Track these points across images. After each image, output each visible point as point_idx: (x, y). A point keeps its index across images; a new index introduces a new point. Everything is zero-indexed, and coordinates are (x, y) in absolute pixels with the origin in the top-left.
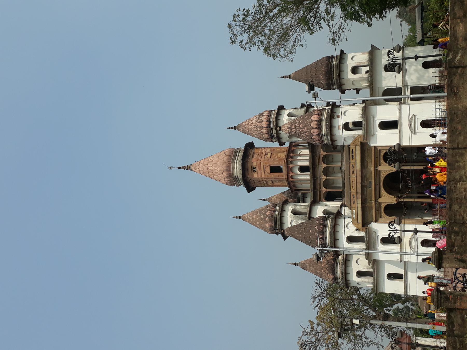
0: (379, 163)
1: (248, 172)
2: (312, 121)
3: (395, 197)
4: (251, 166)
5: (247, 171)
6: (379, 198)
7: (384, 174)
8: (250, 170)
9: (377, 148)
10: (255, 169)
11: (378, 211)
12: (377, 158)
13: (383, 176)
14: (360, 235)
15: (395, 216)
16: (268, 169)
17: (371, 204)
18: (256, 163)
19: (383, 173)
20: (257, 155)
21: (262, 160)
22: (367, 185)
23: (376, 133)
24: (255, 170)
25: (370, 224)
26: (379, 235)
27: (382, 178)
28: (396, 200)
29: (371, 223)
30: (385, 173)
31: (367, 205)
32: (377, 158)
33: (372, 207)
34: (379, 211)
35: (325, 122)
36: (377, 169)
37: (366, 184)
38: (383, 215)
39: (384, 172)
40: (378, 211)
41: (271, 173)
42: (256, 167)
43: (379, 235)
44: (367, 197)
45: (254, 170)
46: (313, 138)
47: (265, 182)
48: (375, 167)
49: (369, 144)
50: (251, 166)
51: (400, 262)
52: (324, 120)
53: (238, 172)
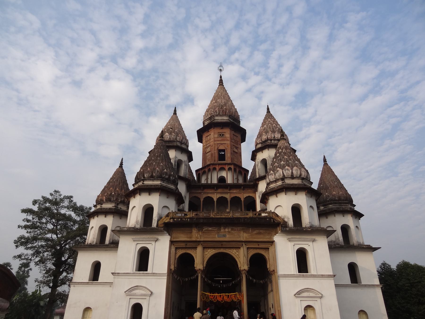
0: (251, 248)
2: (300, 169)
3: (204, 268)
4: (225, 132)
7: (236, 254)
8: (221, 131)
9: (271, 245)
10: (222, 136)
11: (186, 244)
14: (153, 222)
15: (177, 267)
16: (221, 148)
17: (196, 236)
20: (235, 139)
21: (231, 142)
22: (221, 231)
23: (293, 243)
25: (168, 234)
26: (152, 245)
27: (230, 250)
28: (200, 269)
29: (169, 236)
30: (237, 255)
32: (258, 245)
33: (191, 238)
35: (301, 183)
36: (242, 245)
37: (222, 230)
38: (180, 251)
40: (186, 244)
41: (218, 150)
42: (225, 137)
43: (152, 245)
44: (204, 231)
45: (221, 135)
46: (278, 169)
47: (208, 145)
48: (246, 242)
49: (276, 235)
50: (225, 132)
51: (112, 273)
52: (302, 182)
53: (219, 119)
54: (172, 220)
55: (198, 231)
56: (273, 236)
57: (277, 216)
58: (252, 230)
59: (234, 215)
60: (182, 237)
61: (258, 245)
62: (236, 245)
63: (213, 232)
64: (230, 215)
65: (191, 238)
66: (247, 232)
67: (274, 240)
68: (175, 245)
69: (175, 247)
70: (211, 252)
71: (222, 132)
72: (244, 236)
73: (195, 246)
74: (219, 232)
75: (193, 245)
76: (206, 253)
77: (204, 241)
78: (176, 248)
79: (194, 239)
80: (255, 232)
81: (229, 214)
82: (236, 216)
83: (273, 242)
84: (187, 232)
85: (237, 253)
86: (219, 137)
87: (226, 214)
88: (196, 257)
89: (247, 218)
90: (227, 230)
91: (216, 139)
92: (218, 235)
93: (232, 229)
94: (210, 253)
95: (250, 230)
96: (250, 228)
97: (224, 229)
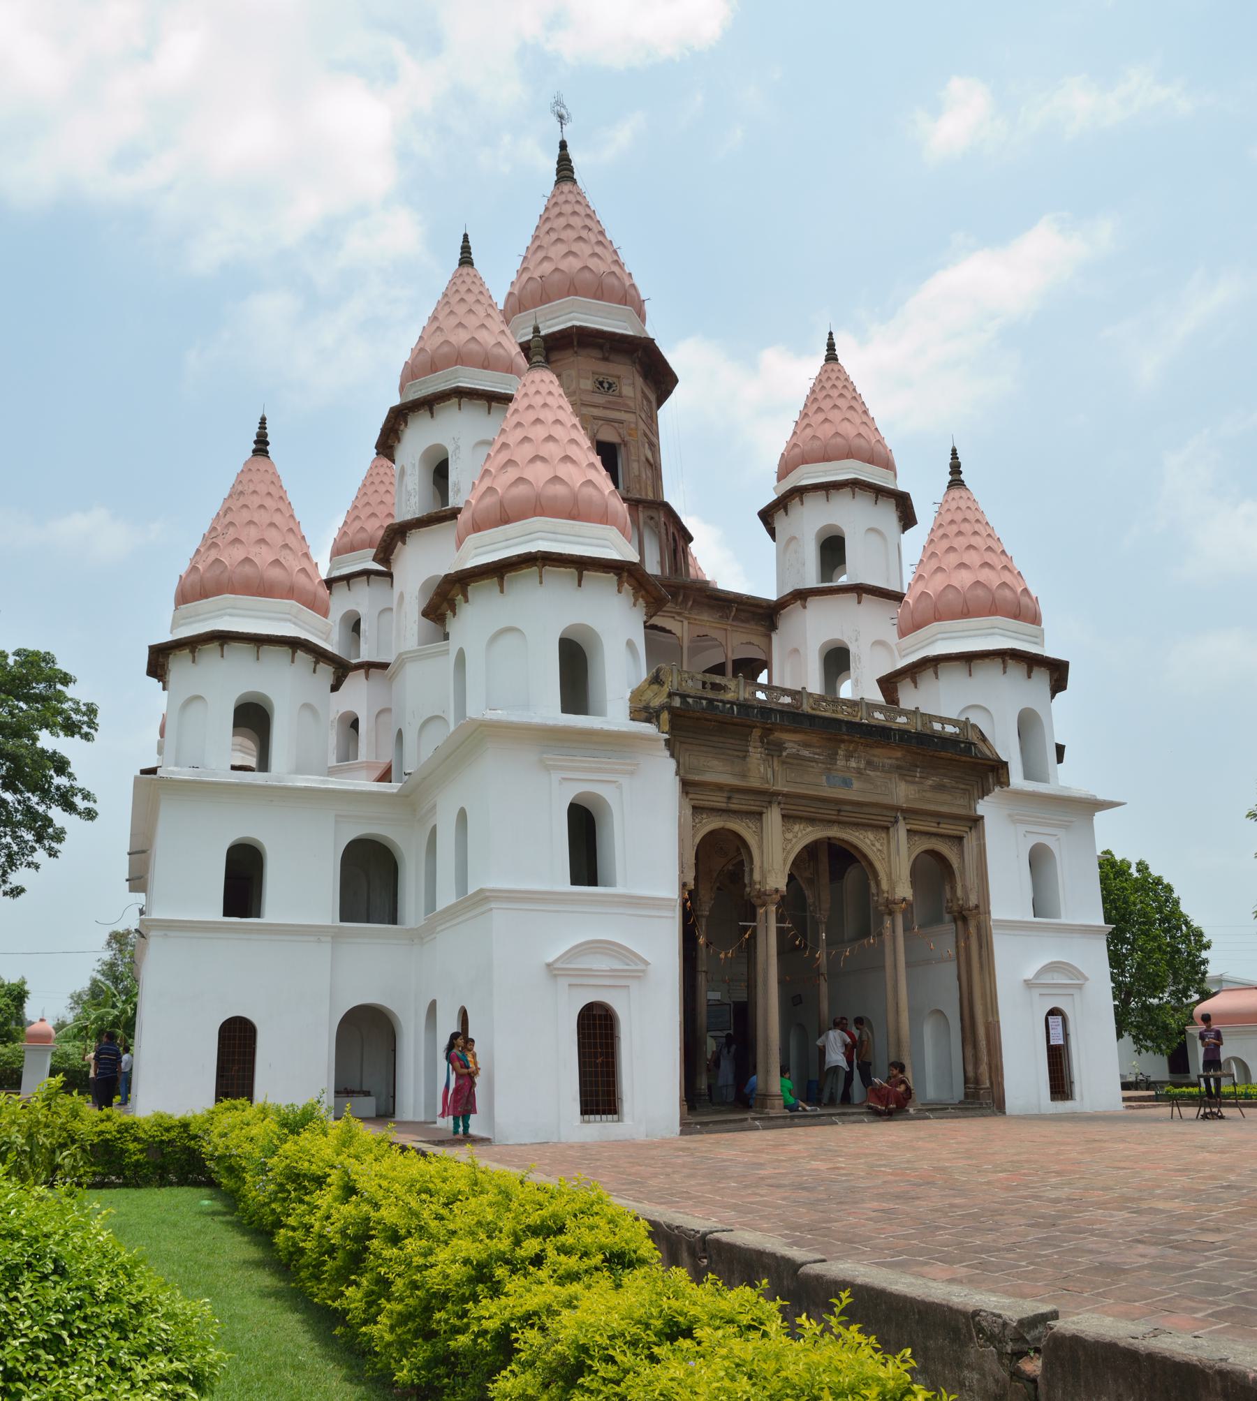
1: (596, 358)
4: (619, 377)
5: (600, 356)
6: (785, 812)
7: (874, 849)
8: (603, 368)
9: (971, 828)
10: (609, 389)
11: (729, 798)
12: (939, 823)
13: (866, 841)
17: (760, 772)
18: (633, 396)
19: (877, 844)
22: (836, 764)
24: (604, 388)
25: (667, 753)
27: (857, 834)
30: (879, 850)
31: (756, 754)
32: (939, 823)
34: (725, 805)
37: (838, 762)
39: (880, 848)
40: (729, 798)
43: (620, 787)
45: (603, 385)
49: (982, 798)
54: (677, 702)
55: (767, 755)
56: (976, 803)
57: (984, 739)
58: (923, 775)
59: (869, 715)
60: (717, 772)
61: (936, 825)
62: (880, 818)
63: (813, 767)
64: (859, 714)
65: (744, 776)
66: (910, 779)
67: (980, 812)
68: (691, 796)
69: (693, 802)
70: (804, 832)
71: (607, 375)
72: (902, 792)
73: (757, 806)
74: (829, 769)
75: (752, 802)
76: (789, 836)
77: (786, 795)
78: (696, 809)
79: (755, 783)
80: (930, 782)
81: (856, 709)
82: (877, 721)
83: (978, 820)
84: (730, 752)
85: (878, 845)
86: (597, 390)
87: (849, 710)
88: (761, 847)
89: (910, 732)
90: (853, 764)
91: (588, 398)
92: (828, 778)
93: (869, 763)
94: (806, 835)
95: (918, 775)
96: (917, 767)
97: (847, 761)
